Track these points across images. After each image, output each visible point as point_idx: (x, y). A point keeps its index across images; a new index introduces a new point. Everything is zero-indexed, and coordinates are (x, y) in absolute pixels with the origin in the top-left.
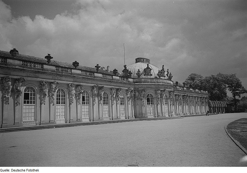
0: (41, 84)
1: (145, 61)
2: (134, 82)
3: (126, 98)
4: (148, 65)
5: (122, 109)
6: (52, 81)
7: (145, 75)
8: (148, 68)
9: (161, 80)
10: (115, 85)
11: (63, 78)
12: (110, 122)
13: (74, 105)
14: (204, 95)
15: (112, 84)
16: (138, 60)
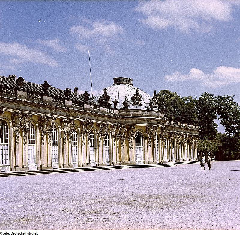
0: (41, 120)
1: (128, 82)
2: (121, 115)
3: (111, 137)
4: (137, 91)
5: (108, 153)
6: (50, 115)
7: (133, 105)
8: (137, 95)
9: (154, 113)
10: (102, 119)
11: (59, 112)
12: (60, 171)
13: (44, 147)
14: (193, 132)
15: (100, 118)
16: (117, 81)
